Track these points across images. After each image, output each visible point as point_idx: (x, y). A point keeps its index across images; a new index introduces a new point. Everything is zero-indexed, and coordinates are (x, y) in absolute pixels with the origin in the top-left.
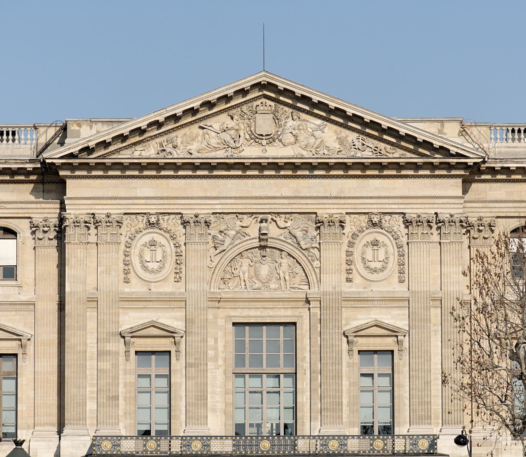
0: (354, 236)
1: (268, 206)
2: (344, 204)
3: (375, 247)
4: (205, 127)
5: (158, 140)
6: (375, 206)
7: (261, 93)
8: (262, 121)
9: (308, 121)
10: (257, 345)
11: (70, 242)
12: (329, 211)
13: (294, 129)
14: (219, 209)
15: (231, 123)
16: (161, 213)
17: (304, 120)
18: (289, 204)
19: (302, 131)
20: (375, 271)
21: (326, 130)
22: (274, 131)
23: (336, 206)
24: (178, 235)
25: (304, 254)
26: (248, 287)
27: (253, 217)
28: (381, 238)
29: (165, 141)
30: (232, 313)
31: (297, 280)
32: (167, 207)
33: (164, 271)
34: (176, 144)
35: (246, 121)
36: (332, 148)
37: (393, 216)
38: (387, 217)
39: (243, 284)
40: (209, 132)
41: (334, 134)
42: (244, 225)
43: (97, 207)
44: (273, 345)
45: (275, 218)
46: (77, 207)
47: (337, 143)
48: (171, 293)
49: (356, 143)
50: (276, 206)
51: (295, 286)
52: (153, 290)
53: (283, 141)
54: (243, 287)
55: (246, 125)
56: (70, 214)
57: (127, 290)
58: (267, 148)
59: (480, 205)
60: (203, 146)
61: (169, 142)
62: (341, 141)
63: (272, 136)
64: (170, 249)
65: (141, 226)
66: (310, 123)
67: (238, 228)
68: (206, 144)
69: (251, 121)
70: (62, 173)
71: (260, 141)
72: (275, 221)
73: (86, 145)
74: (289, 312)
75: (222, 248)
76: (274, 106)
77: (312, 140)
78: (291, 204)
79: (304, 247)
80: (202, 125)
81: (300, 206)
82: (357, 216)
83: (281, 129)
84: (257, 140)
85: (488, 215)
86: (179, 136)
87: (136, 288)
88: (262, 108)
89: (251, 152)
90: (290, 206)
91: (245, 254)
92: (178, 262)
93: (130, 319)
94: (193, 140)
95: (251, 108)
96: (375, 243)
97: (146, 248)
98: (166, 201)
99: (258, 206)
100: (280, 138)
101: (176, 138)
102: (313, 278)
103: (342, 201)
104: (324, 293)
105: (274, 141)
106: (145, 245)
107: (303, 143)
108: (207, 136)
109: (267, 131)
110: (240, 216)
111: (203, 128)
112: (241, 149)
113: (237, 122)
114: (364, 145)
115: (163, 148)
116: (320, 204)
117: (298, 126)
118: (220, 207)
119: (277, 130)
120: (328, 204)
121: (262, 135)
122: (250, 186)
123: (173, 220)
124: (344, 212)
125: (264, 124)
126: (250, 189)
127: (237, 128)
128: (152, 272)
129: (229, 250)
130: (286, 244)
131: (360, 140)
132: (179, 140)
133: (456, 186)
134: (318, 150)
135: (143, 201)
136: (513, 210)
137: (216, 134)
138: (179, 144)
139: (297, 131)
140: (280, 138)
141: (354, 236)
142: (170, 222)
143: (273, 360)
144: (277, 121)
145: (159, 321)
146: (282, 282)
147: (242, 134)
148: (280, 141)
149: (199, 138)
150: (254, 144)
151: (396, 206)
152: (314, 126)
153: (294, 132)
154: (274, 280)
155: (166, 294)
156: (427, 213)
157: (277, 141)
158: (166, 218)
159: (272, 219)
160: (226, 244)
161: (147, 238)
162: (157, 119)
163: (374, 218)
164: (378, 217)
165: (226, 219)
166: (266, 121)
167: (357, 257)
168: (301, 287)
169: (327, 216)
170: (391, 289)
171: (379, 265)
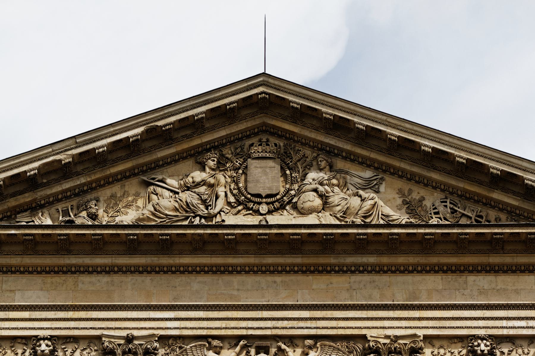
1: (269, 324)
2: (420, 319)
4: (152, 181)
5: (60, 207)
6: (481, 323)
7: (257, 121)
8: (260, 170)
9: (347, 173)
12: (389, 332)
13: (321, 184)
14: (173, 328)
15: (198, 176)
16: (59, 337)
17: (340, 171)
18: (311, 319)
19: (336, 189)
21: (382, 188)
22: (282, 190)
23: (404, 323)
27: (242, 343)
29: (75, 208)
32: (72, 324)
34: (94, 211)
35: (229, 173)
36: (395, 217)
37: (518, 342)
40: (159, 190)
41: (397, 196)
45: (283, 346)
47: (404, 210)
49: (441, 209)
50: (285, 323)
53: (300, 205)
55: (229, 180)
58: (269, 218)
60: (147, 213)
61: (81, 209)
63: (278, 197)
66: (352, 175)
68: (152, 209)
69: (240, 171)
71: (255, 207)
72: (283, 351)
76: (282, 148)
77: (355, 202)
80: (145, 178)
81: (334, 323)
82: (445, 343)
83: (296, 186)
84: (251, 205)
86: (101, 199)
88: (260, 149)
90: (313, 324)
94: (128, 206)
95: (239, 150)
99: (250, 324)
100: (294, 201)
101: (94, 202)
105: (283, 207)
107: (339, 208)
108: (154, 197)
109: (270, 188)
110: (215, 343)
111: (148, 184)
112: (218, 219)
113: (214, 172)
114: (456, 211)
115: (68, 218)
116: (372, 319)
117: (329, 180)
118: (176, 324)
119: (288, 186)
120: (388, 319)
121: (259, 196)
122: (236, 287)
123: (85, 352)
124: (421, 333)
125: (265, 176)
126: (235, 293)
127: (212, 181)
131: (448, 204)
134: (368, 220)
135: (26, 314)
137: (171, 194)
138: (101, 212)
139: (326, 187)
140: (294, 201)
144: (288, 172)
147: (222, 194)
148: (295, 207)
149: (140, 203)
150: (244, 212)
151: (523, 323)
152: (359, 181)
153: (321, 188)
157: (287, 208)
159: (279, 349)
163: (479, 345)
164: (488, 343)
165: (188, 347)
166: (268, 170)
169: (387, 341)
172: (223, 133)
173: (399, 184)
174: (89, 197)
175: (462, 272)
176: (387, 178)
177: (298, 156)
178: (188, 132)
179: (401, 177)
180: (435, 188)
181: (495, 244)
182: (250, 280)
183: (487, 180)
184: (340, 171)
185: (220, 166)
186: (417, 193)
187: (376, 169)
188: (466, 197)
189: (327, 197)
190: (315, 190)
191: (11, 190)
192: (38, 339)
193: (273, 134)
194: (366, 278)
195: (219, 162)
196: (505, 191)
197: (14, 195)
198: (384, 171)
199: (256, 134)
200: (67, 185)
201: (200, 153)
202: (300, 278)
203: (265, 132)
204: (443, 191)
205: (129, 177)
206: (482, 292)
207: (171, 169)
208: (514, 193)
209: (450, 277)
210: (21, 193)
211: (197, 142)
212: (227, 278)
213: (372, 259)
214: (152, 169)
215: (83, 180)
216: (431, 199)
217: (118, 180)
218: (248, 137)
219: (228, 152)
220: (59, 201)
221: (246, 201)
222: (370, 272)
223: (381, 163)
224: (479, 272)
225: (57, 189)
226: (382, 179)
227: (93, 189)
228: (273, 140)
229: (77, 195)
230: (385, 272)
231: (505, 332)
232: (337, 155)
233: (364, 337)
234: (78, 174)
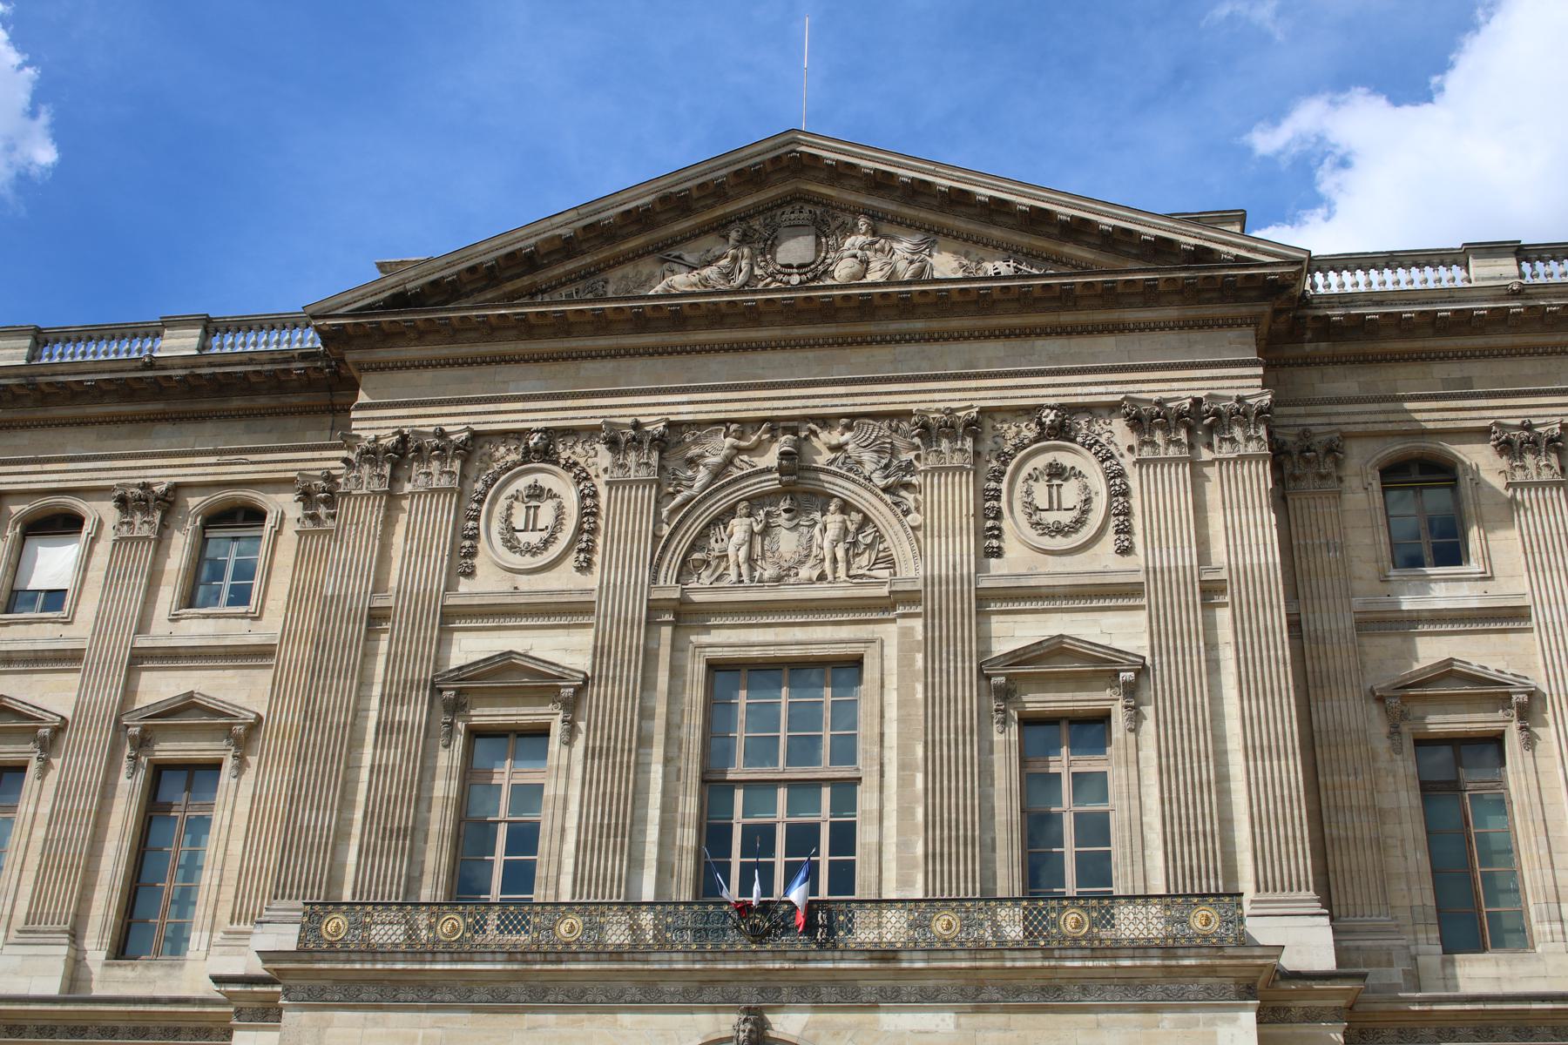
2: (976, 389)
3: (1056, 482)
6: (1051, 391)
10: (764, 716)
11: (349, 494)
12: (941, 406)
16: (556, 430)
18: (847, 395)
19: (879, 255)
20: (1059, 530)
24: (593, 474)
25: (882, 500)
26: (745, 578)
28: (1066, 459)
31: (864, 560)
37: (1096, 411)
39: (733, 572)
40: (675, 267)
42: (743, 444)
43: (418, 422)
44: (804, 716)
46: (376, 424)
48: (562, 592)
51: (860, 572)
54: (734, 577)
56: (358, 437)
59: (1302, 410)
65: (514, 457)
70: (352, 356)
71: (785, 279)
73: (400, 289)
74: (845, 632)
75: (686, 493)
78: (852, 395)
79: (882, 483)
82: (1008, 416)
84: (780, 277)
85: (1321, 429)
92: (586, 526)
96: (1057, 473)
97: (516, 504)
98: (569, 403)
110: (733, 427)
117: (873, 243)
121: (790, 266)
129: (705, 498)
130: (839, 481)
133: (1243, 344)
136: (1382, 417)
142: (578, 449)
143: (804, 750)
145: (531, 654)
146: (827, 565)
153: (859, 253)
154: (811, 562)
155: (551, 593)
156: (1177, 399)
160: (697, 485)
162: (558, 232)
168: (873, 573)
171: (1066, 518)
172: (749, 201)
173: (955, 245)
174: (596, 278)
175: (1028, 335)
176: (940, 239)
177: (837, 223)
178: (709, 202)
179: (956, 238)
180: (996, 247)
181: (1064, 298)
182: (778, 357)
183: (1056, 231)
184: (886, 237)
185: (744, 240)
187: (928, 231)
188: (1031, 256)
189: (868, 263)
190: (855, 256)
191: (508, 274)
192: (530, 431)
193: (808, 201)
194: (912, 348)
195: (745, 235)
196: (1078, 242)
197: (510, 279)
198: (937, 233)
199: (789, 203)
200: (571, 265)
201: (725, 226)
202: (836, 352)
203: (800, 199)
204: (1005, 250)
205: (642, 256)
206: (1053, 358)
207: (692, 245)
208: (1089, 245)
209: (1015, 343)
210: (519, 276)
211: (719, 212)
212: (751, 356)
213: (918, 325)
214: (669, 246)
215: (589, 260)
217: (631, 260)
218: (780, 206)
219: (756, 224)
220: (563, 284)
222: (918, 341)
223: (932, 224)
224: (1048, 334)
225: (559, 270)
226: (934, 242)
227: (601, 270)
228: (807, 208)
229: (583, 278)
230: (936, 340)
231: (1080, 399)
232: (881, 219)
233: (910, 413)
234: (583, 253)
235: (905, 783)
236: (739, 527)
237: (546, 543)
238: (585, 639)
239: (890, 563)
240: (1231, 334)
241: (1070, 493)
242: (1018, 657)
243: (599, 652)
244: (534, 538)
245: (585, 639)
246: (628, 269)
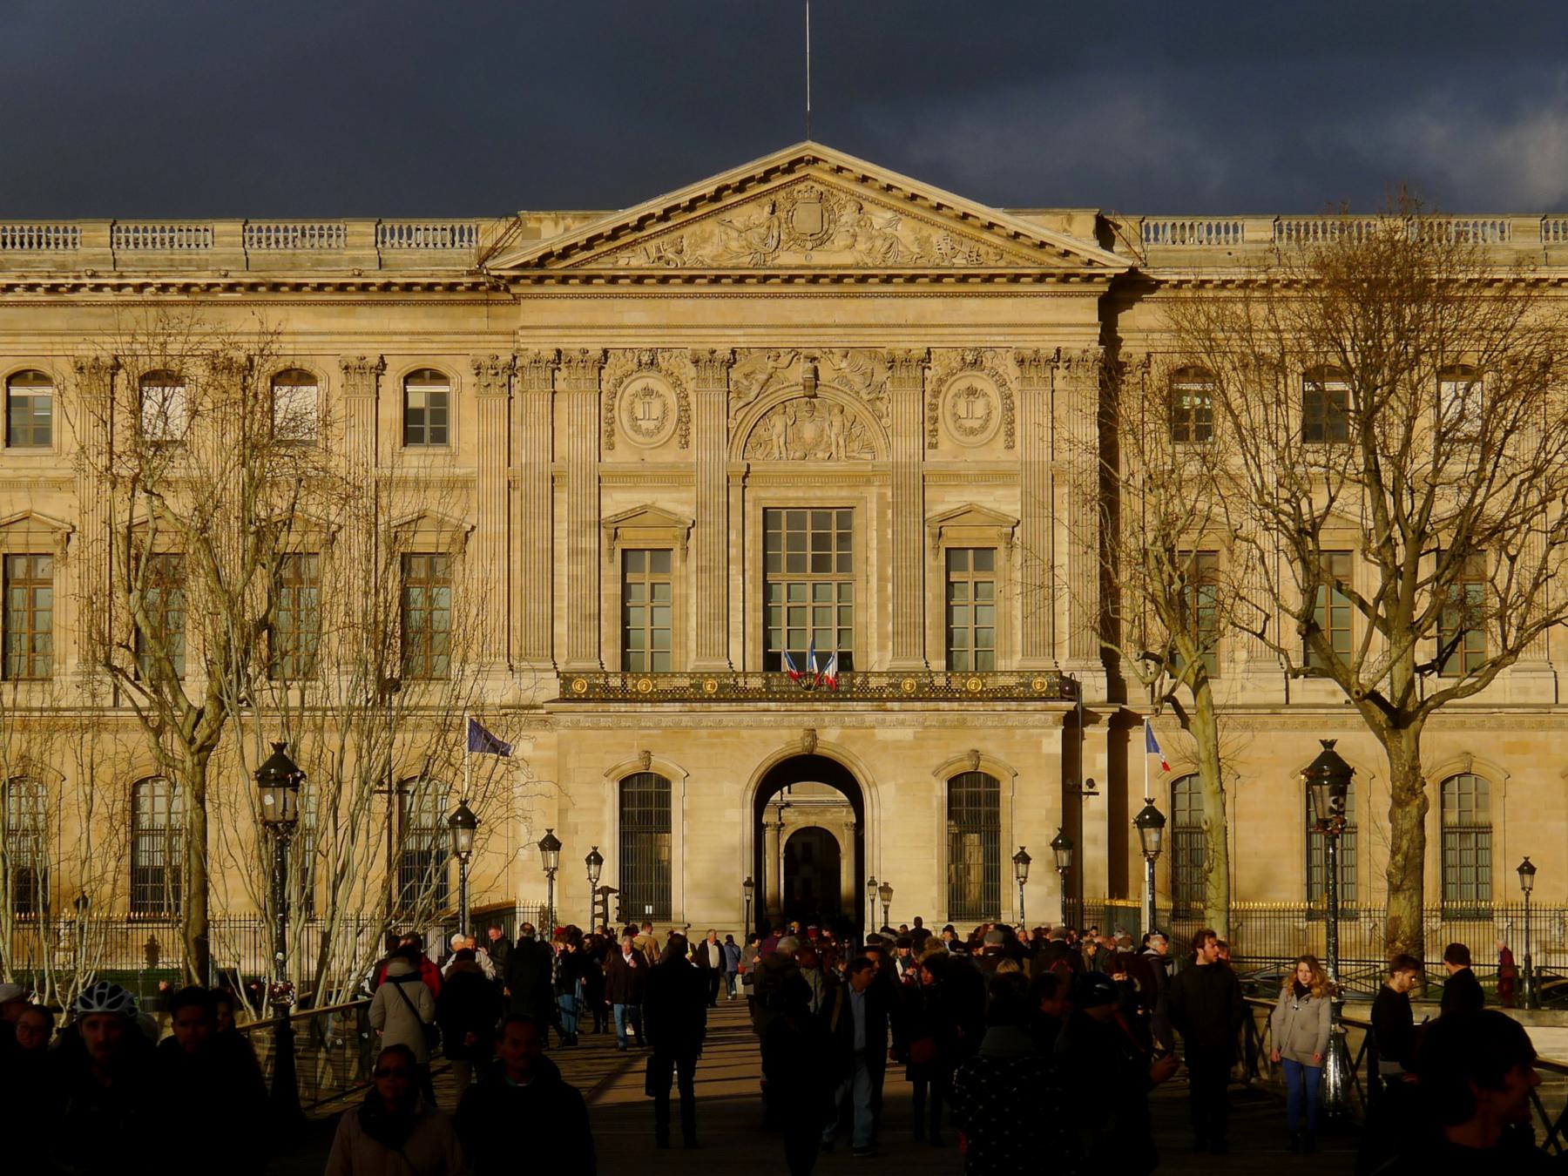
0: (941, 381)
12: (902, 345)
14: (742, 342)
20: (972, 432)
30: (762, 494)
31: (856, 446)
33: (663, 433)
38: (989, 354)
52: (648, 459)
57: (609, 460)
62: (923, 242)
64: (672, 399)
67: (770, 371)
74: (844, 493)
79: (866, 398)
87: (620, 456)
89: (789, 259)
91: (780, 409)
93: (617, 502)
94: (705, 241)
96: (972, 392)
98: (666, 331)
102: (880, 443)
103: (923, 331)
104: (896, 465)
106: (635, 395)
125: (807, 218)
128: (649, 433)
132: (685, 242)
135: (632, 332)
141: (941, 381)
146: (834, 448)
154: (823, 446)
158: (667, 355)
161: (637, 386)
167: (944, 412)
170: (993, 458)
171: (976, 424)
173: (913, 223)
186: (926, 231)
216: (937, 236)
221: (797, 240)
235: (881, 589)
236: (778, 422)
237: (658, 429)
238: (690, 495)
239: (872, 450)
240: (1083, 301)
241: (979, 408)
242: (946, 518)
243: (701, 506)
244: (651, 425)
245: (690, 495)
246: (695, 228)
